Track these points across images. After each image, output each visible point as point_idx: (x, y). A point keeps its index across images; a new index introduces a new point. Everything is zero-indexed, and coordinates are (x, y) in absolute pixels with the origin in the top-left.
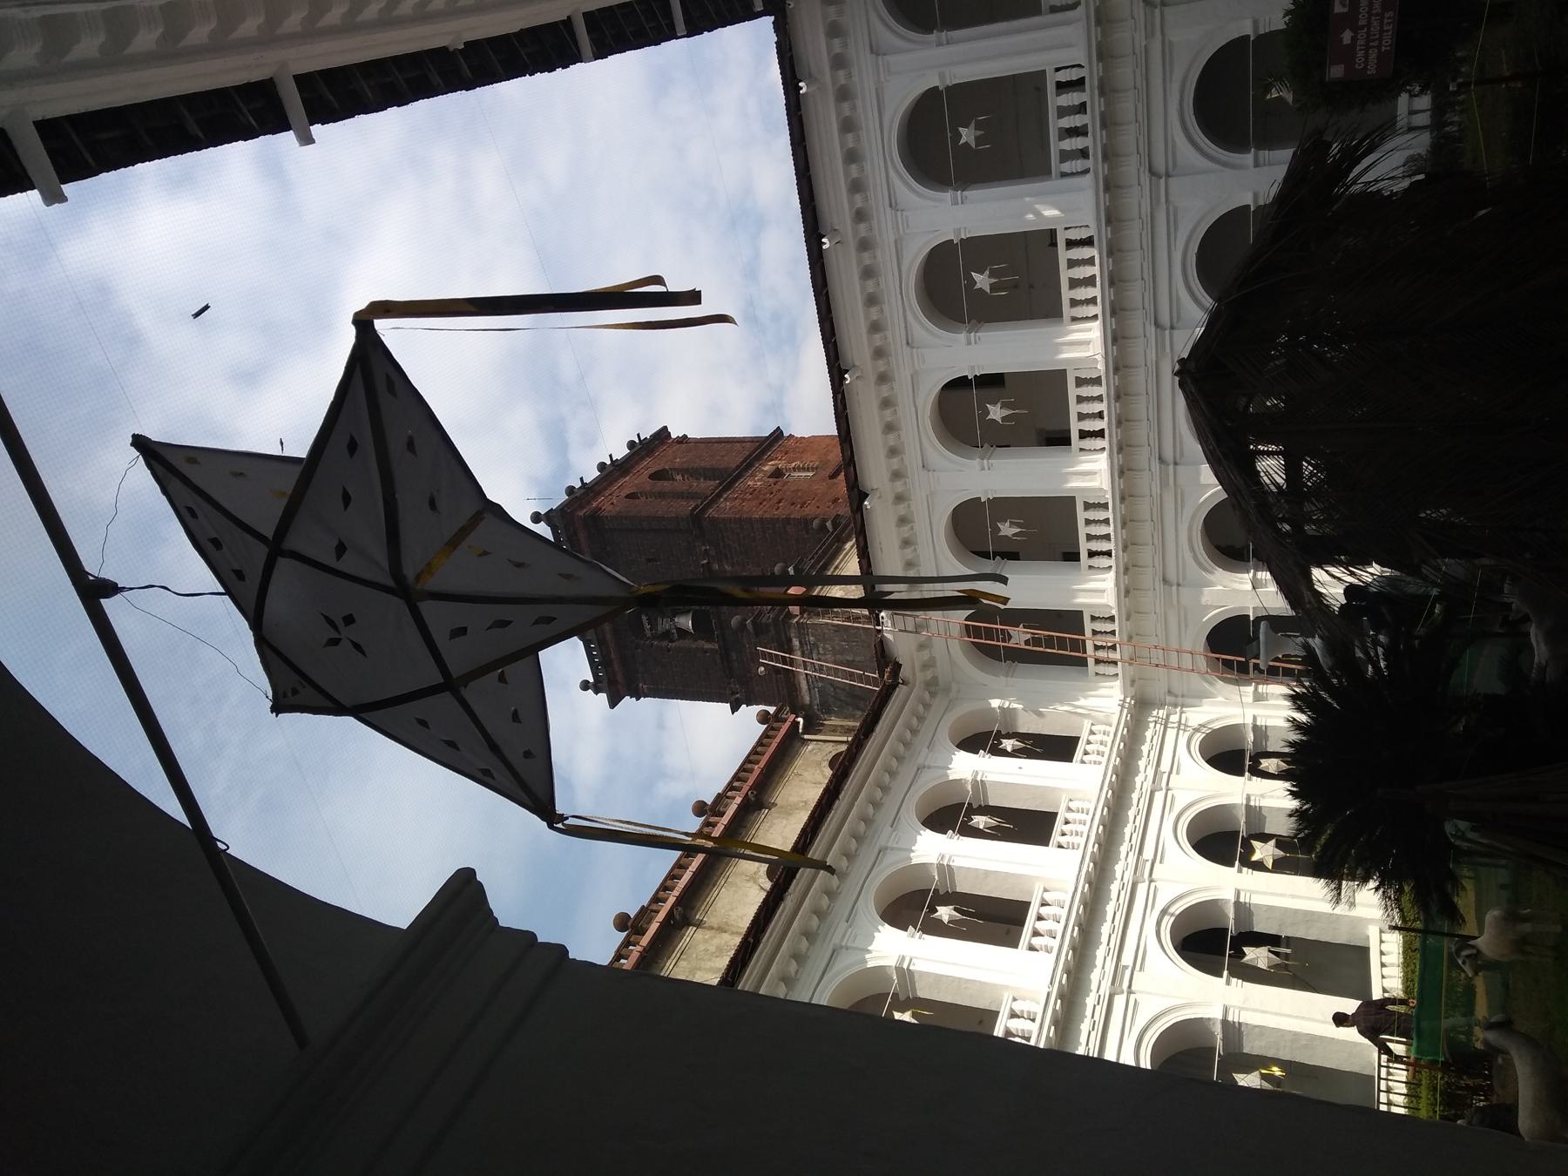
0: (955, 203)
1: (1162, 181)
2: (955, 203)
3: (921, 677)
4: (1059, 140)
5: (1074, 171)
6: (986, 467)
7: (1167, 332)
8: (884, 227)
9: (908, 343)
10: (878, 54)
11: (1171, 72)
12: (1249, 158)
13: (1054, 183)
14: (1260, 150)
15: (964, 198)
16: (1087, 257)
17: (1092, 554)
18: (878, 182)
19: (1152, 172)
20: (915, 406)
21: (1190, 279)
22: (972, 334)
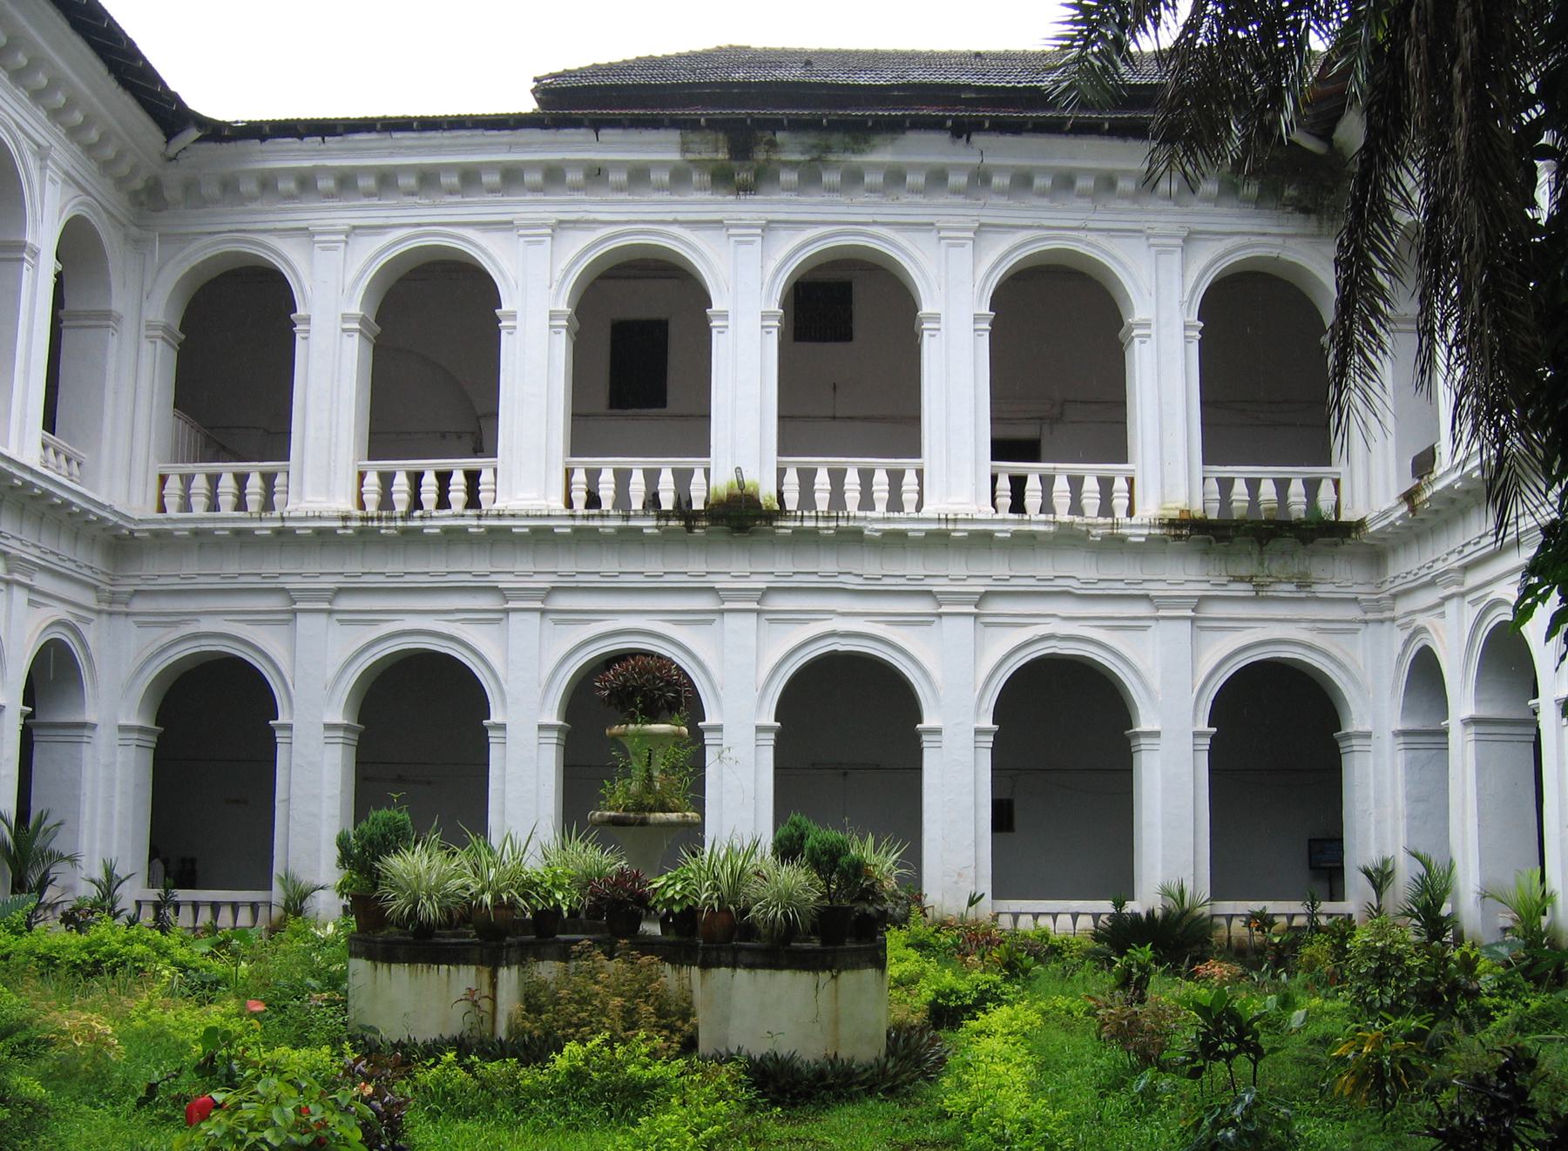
0: (765, 316)
1: (972, 609)
2: (977, 318)
3: (173, 176)
4: (887, 471)
5: (997, 493)
6: (555, 323)
7: (972, 609)
8: (954, 212)
9: (770, 222)
10: (1186, 240)
11: (889, 623)
12: (987, 722)
13: (987, 465)
14: (777, 735)
15: (769, 330)
16: (1028, 502)
17: (187, 480)
18: (1123, 217)
19: (986, 595)
20: (675, 222)
21: (1300, 650)
22: (777, 323)
